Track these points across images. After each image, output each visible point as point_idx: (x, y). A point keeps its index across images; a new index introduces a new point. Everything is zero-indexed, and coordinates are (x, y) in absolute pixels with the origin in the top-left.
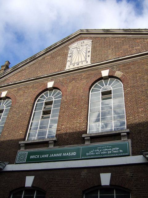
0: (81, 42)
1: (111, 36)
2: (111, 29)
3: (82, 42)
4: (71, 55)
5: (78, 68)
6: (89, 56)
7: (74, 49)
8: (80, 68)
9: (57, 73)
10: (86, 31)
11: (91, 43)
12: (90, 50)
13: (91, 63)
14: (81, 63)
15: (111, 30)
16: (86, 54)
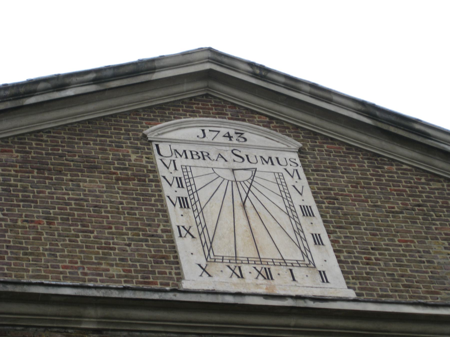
0: (224, 131)
1: (412, 159)
2: (417, 121)
3: (232, 133)
4: (183, 193)
5: (301, 304)
6: (318, 240)
7: (190, 162)
8: (311, 304)
9: (156, 296)
10: (249, 69)
11: (295, 156)
12: (310, 201)
13: (352, 294)
14: (284, 271)
15: (417, 127)
16: (292, 216)
